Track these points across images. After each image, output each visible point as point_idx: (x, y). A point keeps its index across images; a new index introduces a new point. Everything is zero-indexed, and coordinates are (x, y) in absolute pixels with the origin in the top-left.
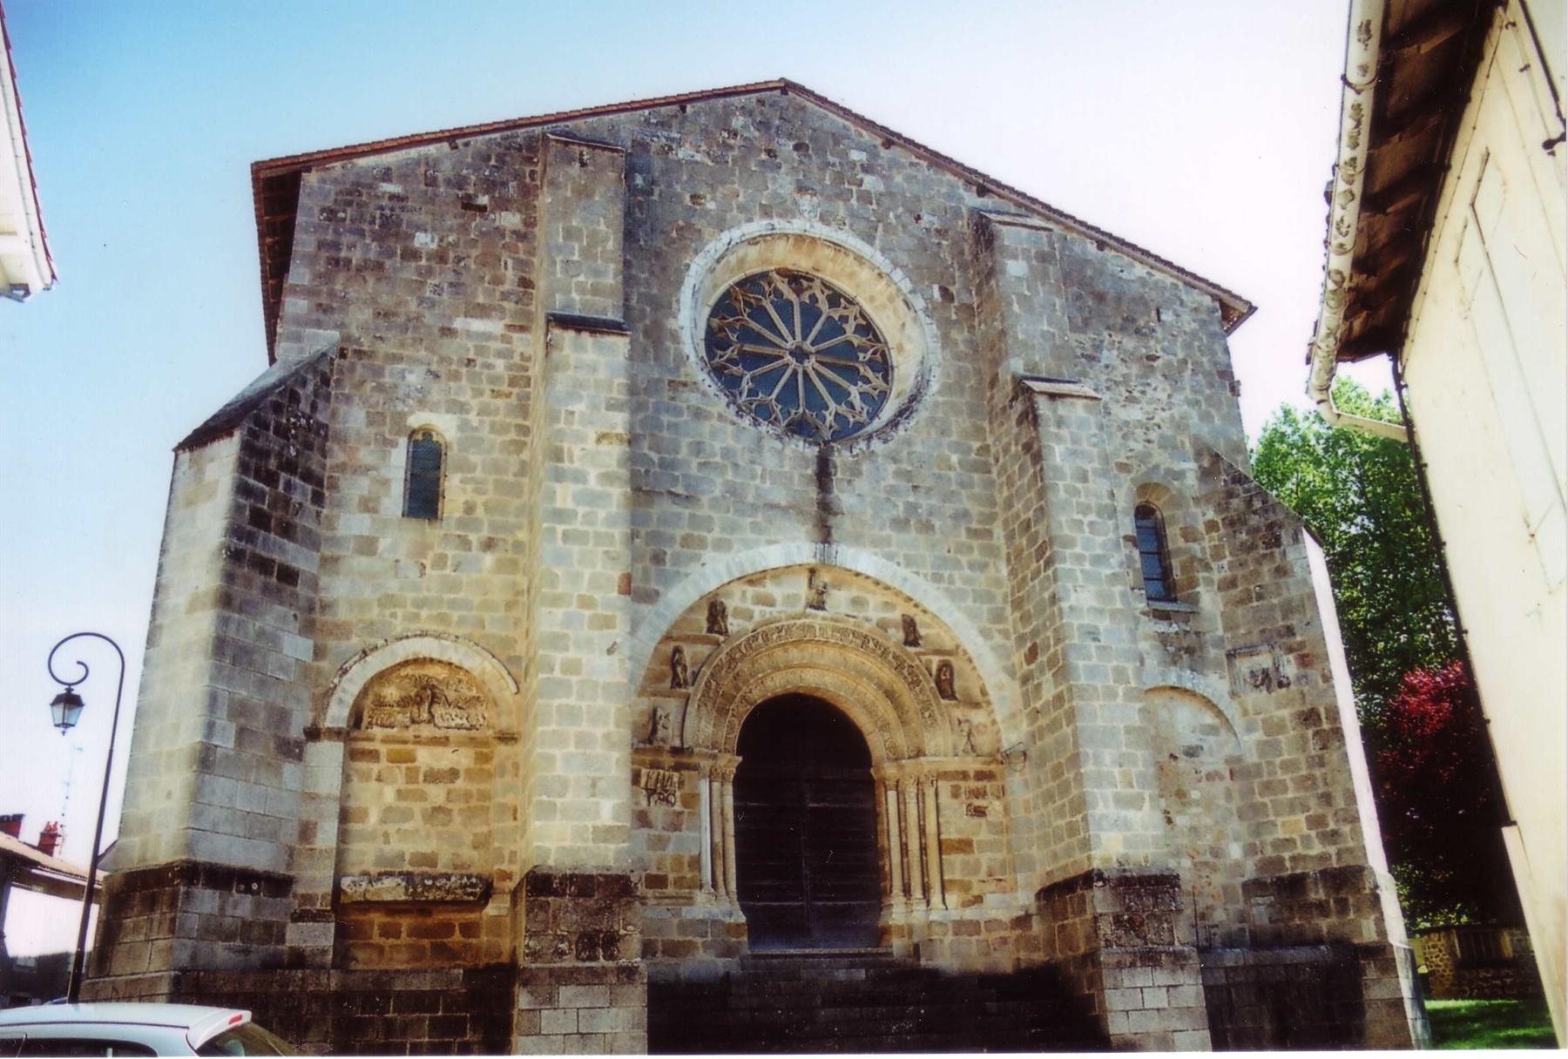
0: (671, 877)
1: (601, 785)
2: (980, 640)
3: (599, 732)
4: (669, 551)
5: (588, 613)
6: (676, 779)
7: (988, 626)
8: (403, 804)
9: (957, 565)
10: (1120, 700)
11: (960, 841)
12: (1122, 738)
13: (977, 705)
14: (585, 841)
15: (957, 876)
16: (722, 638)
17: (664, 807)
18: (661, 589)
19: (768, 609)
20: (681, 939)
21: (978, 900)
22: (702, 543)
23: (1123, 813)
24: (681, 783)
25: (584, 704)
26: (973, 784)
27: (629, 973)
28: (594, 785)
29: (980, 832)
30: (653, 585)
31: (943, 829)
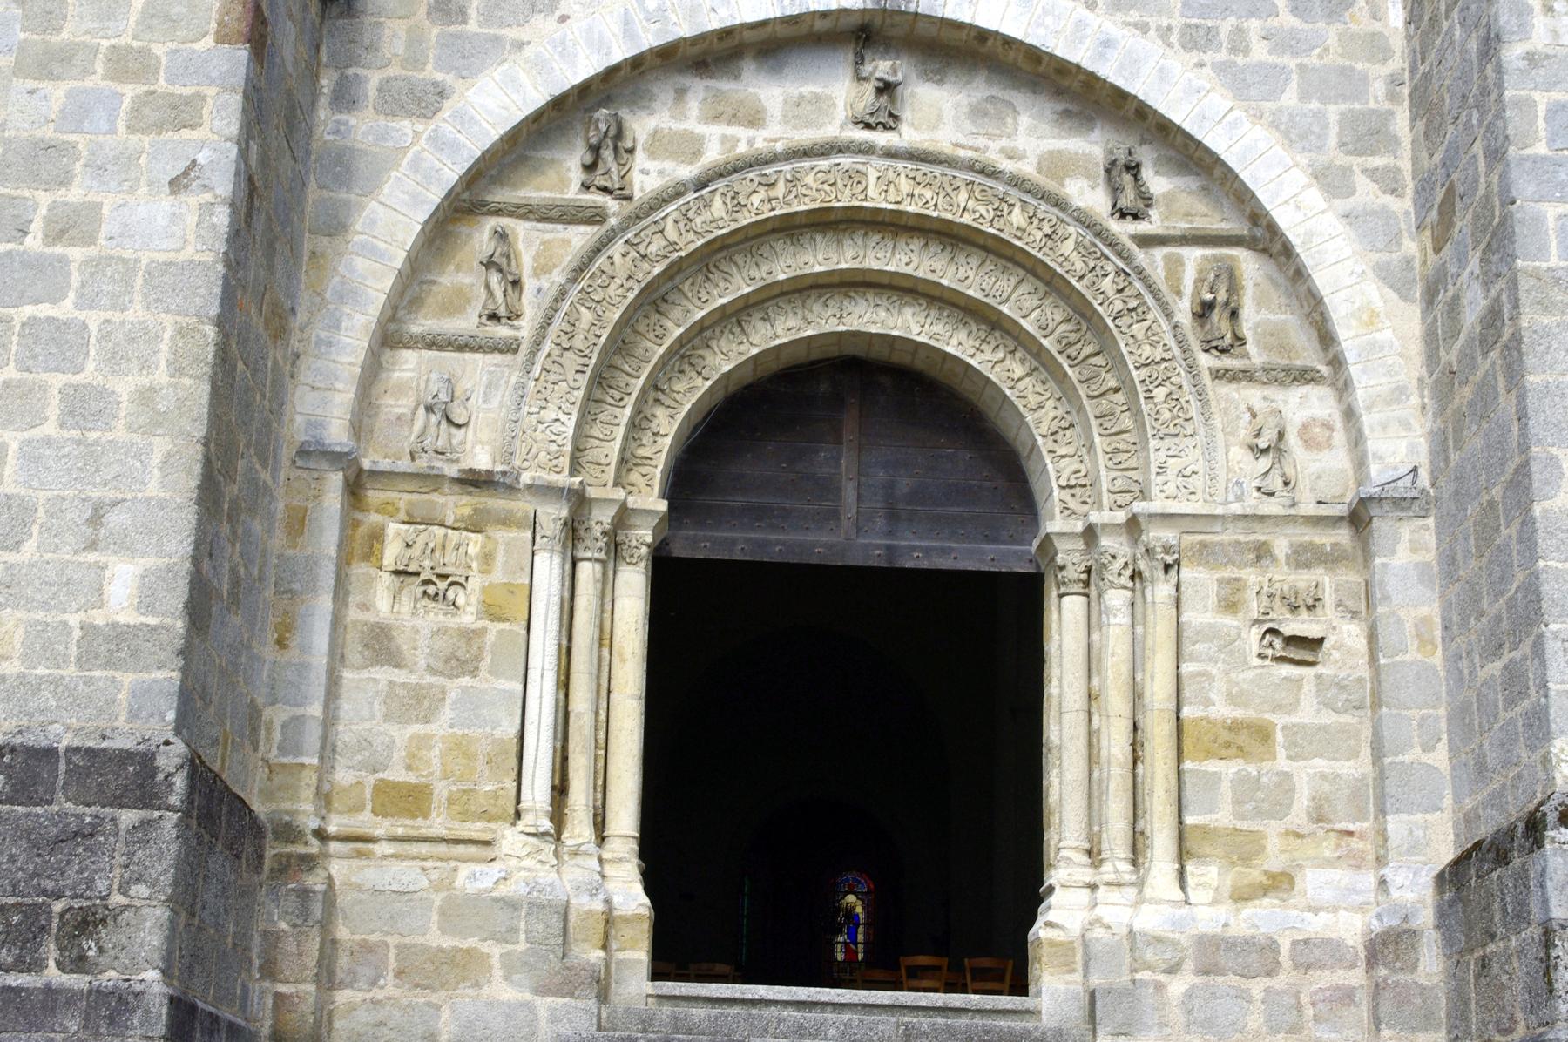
0: (441, 790)
1: (116, 520)
3: (124, 387)
5: (130, 91)
6: (473, 550)
7: (1342, 159)
11: (1235, 727)
13: (1304, 376)
14: (58, 660)
15: (1222, 816)
16: (612, 205)
17: (435, 616)
18: (447, 78)
19: (743, 133)
20: (448, 943)
24: (487, 558)
25: (94, 320)
26: (1284, 577)
28: (96, 519)
29: (1303, 702)
30: (432, 73)
31: (1187, 692)
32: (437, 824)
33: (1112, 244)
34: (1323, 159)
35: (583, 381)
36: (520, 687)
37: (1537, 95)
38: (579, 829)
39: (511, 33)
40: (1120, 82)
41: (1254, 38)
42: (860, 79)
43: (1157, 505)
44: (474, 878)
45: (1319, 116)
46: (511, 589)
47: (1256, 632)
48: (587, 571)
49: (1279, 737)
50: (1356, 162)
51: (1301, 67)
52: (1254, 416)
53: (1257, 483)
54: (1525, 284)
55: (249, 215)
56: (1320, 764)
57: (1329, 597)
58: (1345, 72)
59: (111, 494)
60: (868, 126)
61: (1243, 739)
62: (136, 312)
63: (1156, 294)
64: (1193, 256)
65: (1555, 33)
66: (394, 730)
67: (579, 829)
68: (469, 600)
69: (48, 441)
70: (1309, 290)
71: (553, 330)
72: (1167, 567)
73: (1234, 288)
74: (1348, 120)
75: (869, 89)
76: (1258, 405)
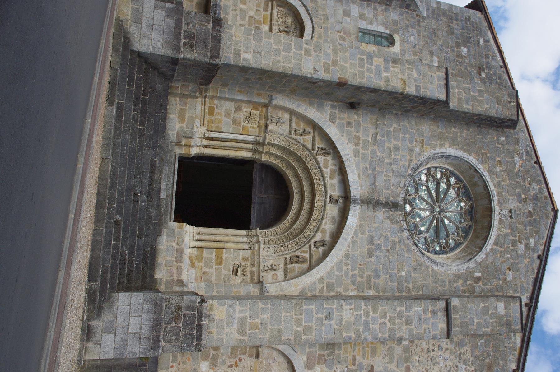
0: (213, 118)
1: (258, 56)
2: (318, 277)
3: (280, 58)
4: (352, 129)
5: (330, 63)
6: (255, 125)
7: (325, 282)
8: (247, 18)
9: (353, 269)
10: (295, 328)
11: (221, 258)
12: (276, 327)
13: (286, 275)
14: (235, 45)
16: (315, 152)
17: (243, 118)
18: (337, 123)
20: (186, 117)
21: (193, 265)
22: (357, 145)
23: (236, 321)
24: (253, 128)
25: (292, 54)
26: (249, 269)
27: (177, 49)
28: (258, 52)
30: (337, 121)
32: (207, 117)
33: (310, 240)
34: (325, 278)
35: (284, 146)
36: (230, 132)
37: (335, 306)
38: (205, 142)
39: (345, 135)
40: (339, 242)
41: (347, 267)
42: (339, 197)
43: (262, 246)
44: (197, 122)
45: (333, 278)
46: (248, 131)
47: (239, 263)
48: (251, 146)
49: (219, 267)
50: (325, 285)
51: (342, 275)
54: (300, 301)
55: (310, 82)
56: (214, 274)
57: (245, 277)
58: (341, 284)
59: (262, 55)
60: (330, 198)
61: (219, 260)
62: (293, 61)
63: (301, 248)
64: (307, 255)
65: (346, 310)
66: (223, 110)
67: (205, 142)
68: (246, 124)
69: (271, 46)
71: (293, 141)
72: (250, 248)
74: (332, 284)
75: (337, 198)
76: (281, 266)
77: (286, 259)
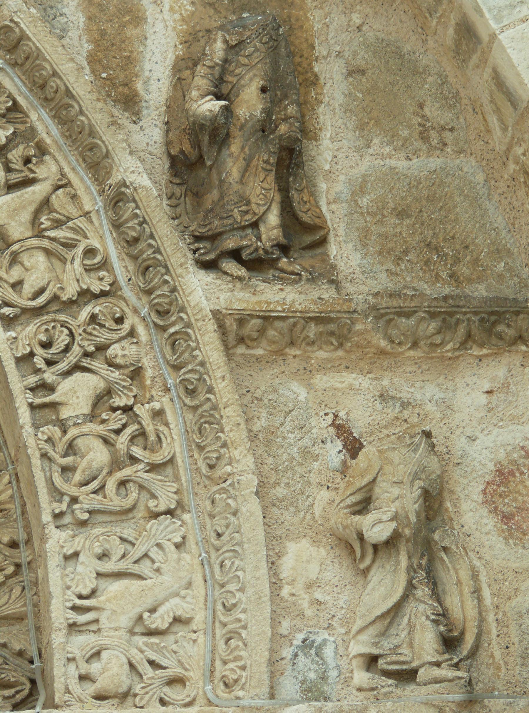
52: (353, 447)
53: (361, 646)
70: (498, 81)
73: (290, 78)
76: (361, 416)
77: (239, 332)
